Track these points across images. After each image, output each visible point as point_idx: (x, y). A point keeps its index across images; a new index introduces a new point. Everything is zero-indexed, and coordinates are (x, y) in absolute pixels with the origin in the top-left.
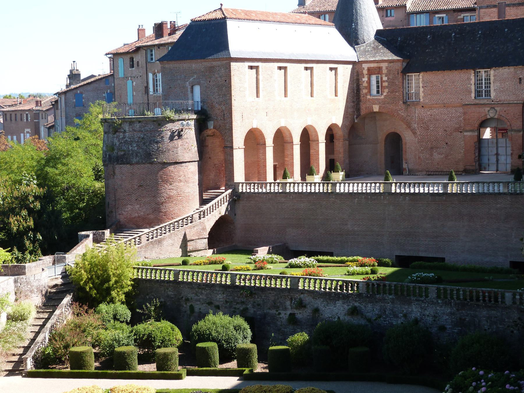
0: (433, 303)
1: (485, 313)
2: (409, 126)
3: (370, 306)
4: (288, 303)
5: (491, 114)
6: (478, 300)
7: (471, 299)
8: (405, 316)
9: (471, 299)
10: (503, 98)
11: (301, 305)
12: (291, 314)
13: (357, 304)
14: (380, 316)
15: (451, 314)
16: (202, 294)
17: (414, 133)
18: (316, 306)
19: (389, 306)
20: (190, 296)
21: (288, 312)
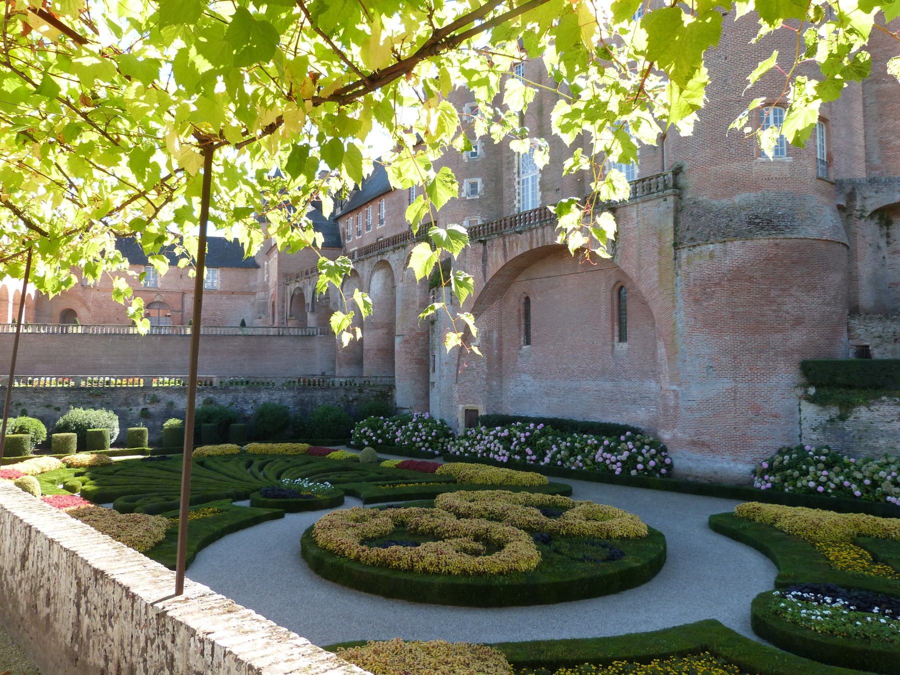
0: (279, 389)
1: (320, 393)
2: (84, 304)
3: (223, 396)
4: (141, 400)
5: (158, 299)
6: (314, 385)
7: (309, 385)
8: (255, 401)
9: (309, 385)
10: (168, 287)
11: (155, 400)
12: (143, 409)
13: (211, 396)
14: (232, 404)
15: (293, 396)
16: (39, 397)
17: (89, 310)
18: (170, 400)
19: (241, 395)
20: (22, 401)
21: (141, 408)
